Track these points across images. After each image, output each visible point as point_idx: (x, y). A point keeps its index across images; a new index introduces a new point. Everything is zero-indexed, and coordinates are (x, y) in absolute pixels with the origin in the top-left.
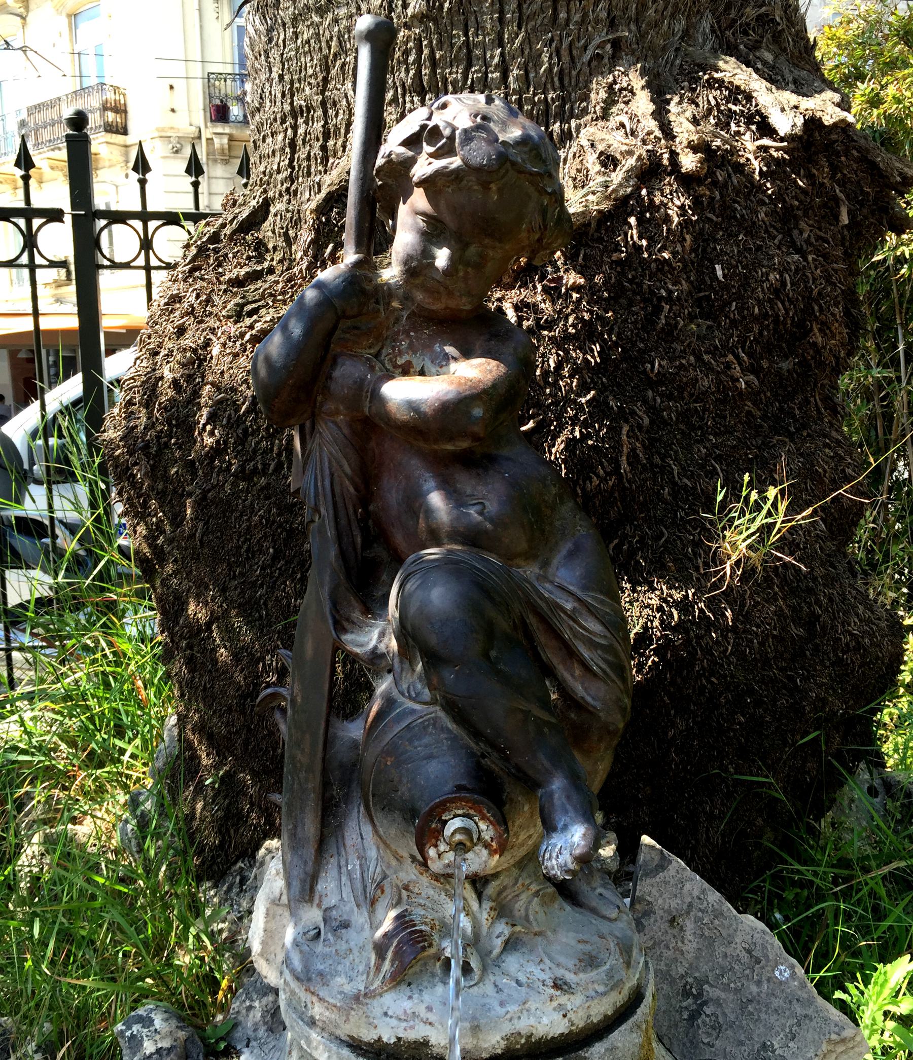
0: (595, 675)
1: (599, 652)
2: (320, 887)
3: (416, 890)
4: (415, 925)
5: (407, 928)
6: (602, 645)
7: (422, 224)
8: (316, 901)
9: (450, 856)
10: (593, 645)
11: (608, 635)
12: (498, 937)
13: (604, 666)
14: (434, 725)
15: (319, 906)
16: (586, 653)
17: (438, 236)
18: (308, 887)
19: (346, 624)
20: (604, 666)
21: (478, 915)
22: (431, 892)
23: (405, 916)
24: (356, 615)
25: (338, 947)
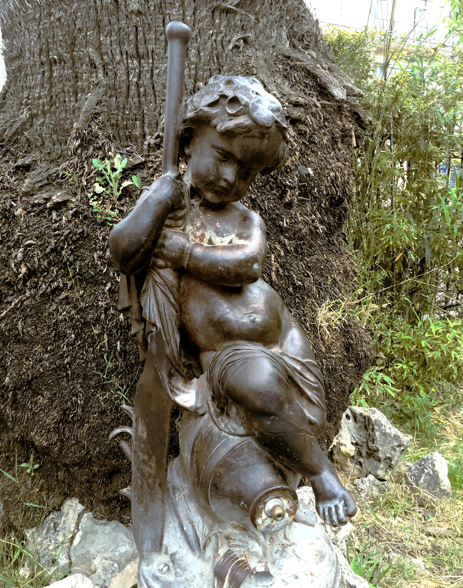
0: (314, 404)
1: (315, 391)
2: (165, 542)
3: (233, 538)
4: (237, 558)
5: (234, 561)
6: (314, 387)
7: (217, 154)
8: (164, 550)
9: (268, 521)
10: (312, 388)
11: (318, 381)
12: (276, 553)
13: (317, 398)
14: (248, 447)
15: (166, 553)
16: (309, 393)
17: (225, 161)
18: (158, 543)
19: (176, 391)
20: (317, 398)
21: (264, 543)
22: (241, 537)
23: (230, 554)
24: (180, 385)
25: (186, 576)
